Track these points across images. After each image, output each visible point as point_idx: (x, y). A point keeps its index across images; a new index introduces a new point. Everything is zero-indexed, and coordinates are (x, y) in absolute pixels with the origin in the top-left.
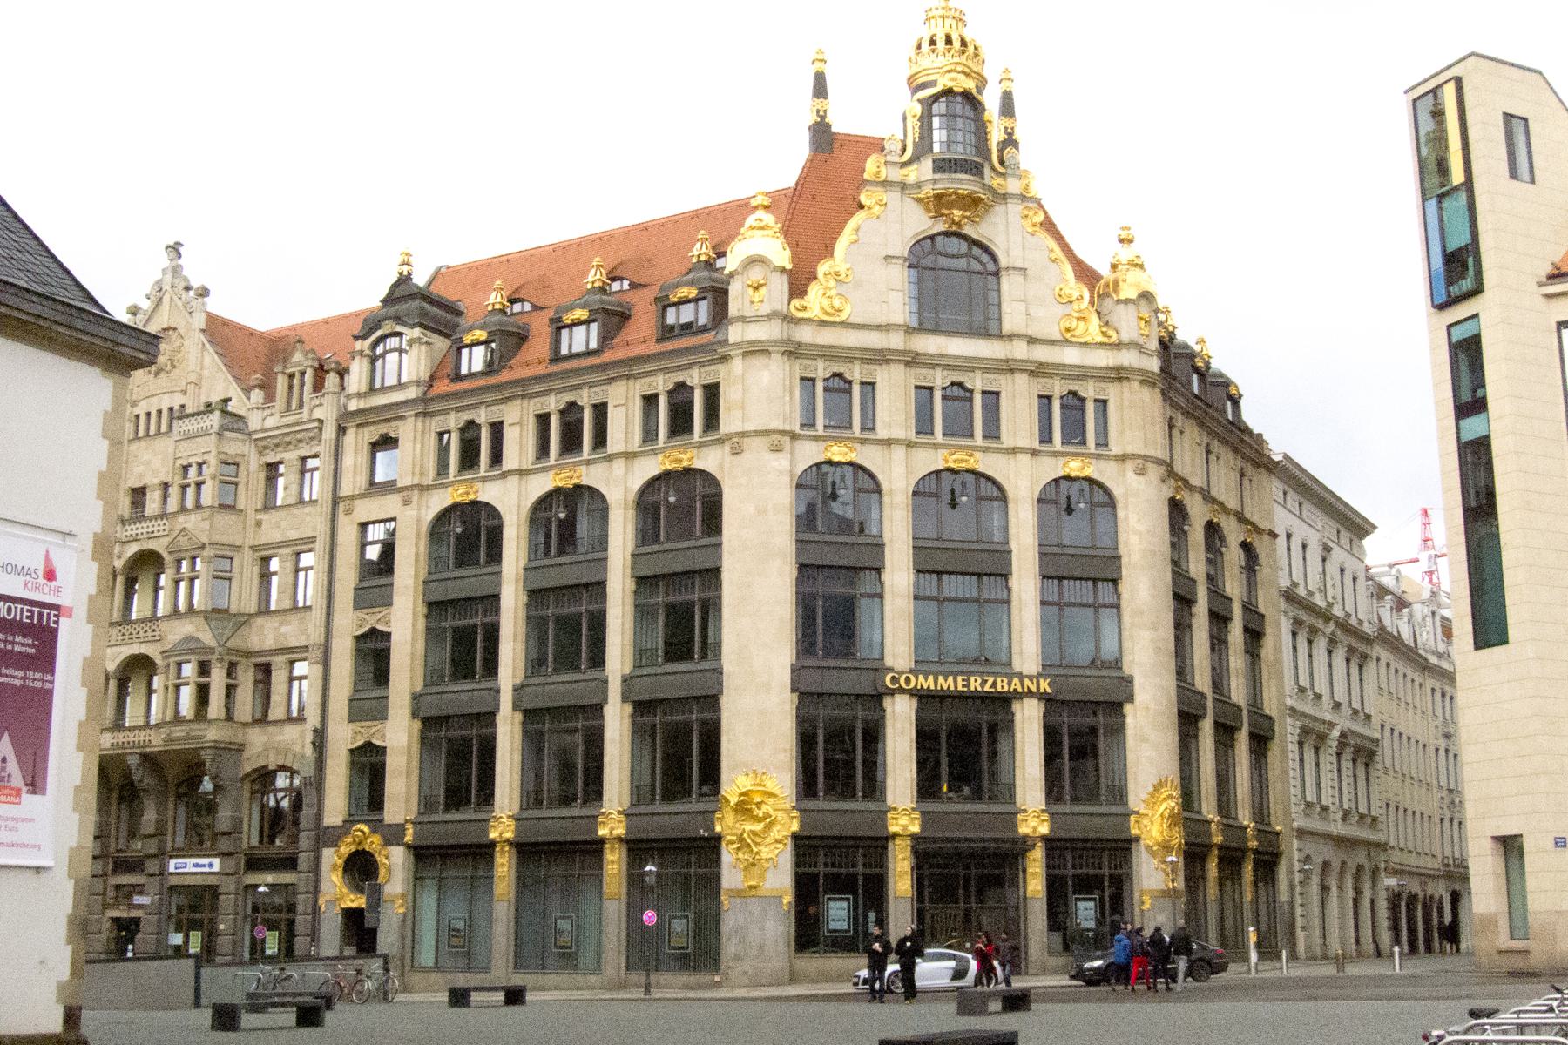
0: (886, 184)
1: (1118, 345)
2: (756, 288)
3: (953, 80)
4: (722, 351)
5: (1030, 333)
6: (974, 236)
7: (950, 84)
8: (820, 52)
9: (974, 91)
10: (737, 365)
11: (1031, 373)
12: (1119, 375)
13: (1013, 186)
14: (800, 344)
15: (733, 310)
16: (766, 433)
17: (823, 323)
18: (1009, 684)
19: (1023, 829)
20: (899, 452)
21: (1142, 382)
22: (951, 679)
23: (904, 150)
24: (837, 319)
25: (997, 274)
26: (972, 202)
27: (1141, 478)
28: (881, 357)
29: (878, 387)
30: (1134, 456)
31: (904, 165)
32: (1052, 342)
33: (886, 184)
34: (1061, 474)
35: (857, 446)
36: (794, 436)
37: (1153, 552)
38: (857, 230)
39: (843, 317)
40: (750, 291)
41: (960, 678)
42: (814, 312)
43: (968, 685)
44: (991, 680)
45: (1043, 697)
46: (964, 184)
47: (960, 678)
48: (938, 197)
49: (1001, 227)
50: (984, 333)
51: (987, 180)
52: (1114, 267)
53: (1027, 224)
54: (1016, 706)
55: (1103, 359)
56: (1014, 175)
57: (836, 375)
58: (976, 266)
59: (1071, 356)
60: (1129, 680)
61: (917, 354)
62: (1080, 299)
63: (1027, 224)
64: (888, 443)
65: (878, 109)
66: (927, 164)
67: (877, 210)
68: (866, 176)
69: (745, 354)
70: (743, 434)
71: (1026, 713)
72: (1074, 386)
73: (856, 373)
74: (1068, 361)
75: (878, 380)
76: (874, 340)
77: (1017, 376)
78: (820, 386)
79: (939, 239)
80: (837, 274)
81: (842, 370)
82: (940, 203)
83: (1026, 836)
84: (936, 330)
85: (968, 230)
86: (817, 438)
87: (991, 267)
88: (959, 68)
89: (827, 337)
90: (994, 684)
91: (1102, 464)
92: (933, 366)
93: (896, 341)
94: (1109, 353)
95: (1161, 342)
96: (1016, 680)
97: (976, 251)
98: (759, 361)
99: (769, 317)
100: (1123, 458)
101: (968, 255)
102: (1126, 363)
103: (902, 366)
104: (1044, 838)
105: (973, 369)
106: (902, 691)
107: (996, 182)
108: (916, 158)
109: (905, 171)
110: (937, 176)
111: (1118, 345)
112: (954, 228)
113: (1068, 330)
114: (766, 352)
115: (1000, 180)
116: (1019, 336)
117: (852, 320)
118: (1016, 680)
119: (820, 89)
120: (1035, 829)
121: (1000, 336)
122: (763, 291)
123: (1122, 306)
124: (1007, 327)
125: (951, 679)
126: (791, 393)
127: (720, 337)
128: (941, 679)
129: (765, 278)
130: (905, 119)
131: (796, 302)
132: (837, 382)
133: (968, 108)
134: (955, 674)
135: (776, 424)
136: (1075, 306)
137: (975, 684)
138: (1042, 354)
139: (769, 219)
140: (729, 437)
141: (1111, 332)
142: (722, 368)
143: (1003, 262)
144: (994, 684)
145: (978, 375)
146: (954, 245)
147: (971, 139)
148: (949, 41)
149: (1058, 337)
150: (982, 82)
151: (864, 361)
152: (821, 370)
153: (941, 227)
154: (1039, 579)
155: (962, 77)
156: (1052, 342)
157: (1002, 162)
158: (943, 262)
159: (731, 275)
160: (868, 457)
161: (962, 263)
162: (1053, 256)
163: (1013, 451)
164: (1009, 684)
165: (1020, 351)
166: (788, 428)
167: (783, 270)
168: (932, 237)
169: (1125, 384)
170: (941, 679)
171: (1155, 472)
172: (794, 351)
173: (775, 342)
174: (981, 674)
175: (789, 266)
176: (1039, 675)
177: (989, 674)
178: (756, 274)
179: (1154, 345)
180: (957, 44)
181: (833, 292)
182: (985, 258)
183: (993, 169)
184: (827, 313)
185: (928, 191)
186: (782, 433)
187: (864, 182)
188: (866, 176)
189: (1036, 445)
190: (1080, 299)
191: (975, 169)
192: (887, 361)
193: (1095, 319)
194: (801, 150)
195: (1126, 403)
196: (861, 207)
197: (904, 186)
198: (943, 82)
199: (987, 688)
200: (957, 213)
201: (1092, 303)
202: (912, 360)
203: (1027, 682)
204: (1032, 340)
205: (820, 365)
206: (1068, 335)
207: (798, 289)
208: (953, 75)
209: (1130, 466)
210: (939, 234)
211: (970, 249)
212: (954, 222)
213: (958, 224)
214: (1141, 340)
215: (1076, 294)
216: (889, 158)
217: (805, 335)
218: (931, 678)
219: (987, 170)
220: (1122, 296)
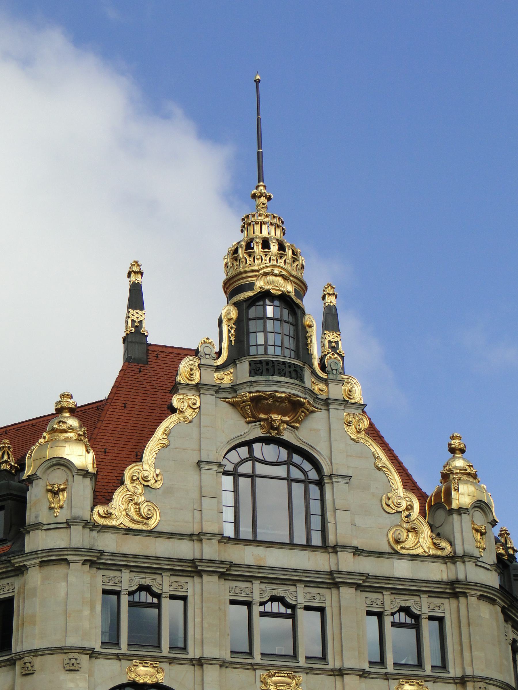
0: (198, 387)
1: (453, 559)
2: (56, 493)
3: (269, 283)
4: (17, 561)
5: (355, 543)
7: (267, 287)
8: (137, 263)
9: (292, 294)
10: (35, 577)
11: (358, 587)
12: (454, 590)
13: (336, 391)
14: (102, 552)
15: (30, 518)
16: (63, 650)
17: (128, 531)
20: (212, 673)
21: (481, 597)
23: (219, 354)
24: (145, 528)
25: (320, 484)
26: (294, 408)
28: (194, 569)
29: (190, 599)
31: (218, 368)
32: (380, 554)
33: (198, 387)
35: (165, 666)
36: (93, 654)
38: (167, 434)
39: (152, 524)
40: (50, 497)
42: (120, 520)
46: (283, 387)
48: (256, 400)
49: (323, 434)
50: (308, 546)
51: (308, 383)
52: (445, 477)
53: (351, 431)
55: (437, 572)
56: (337, 381)
57: (142, 588)
58: (296, 474)
59: (401, 569)
61: (232, 565)
62: (410, 508)
63: (351, 431)
64: (199, 663)
65: (190, 318)
66: (244, 366)
67: (189, 413)
68: (179, 379)
69: (43, 564)
70: (35, 652)
74: (398, 574)
75: (190, 593)
76: (185, 550)
77: (343, 590)
78: (125, 599)
79: (257, 447)
80: (145, 479)
81: (149, 582)
82: (255, 408)
84: (254, 542)
86: (119, 657)
87: (313, 475)
88: (276, 271)
89: (133, 546)
92: (249, 579)
93: (210, 550)
94: (443, 567)
95: (499, 556)
97: (296, 459)
98: (58, 570)
99: (68, 524)
101: (289, 463)
102: (461, 577)
103: (215, 579)
105: (294, 582)
107: (317, 387)
108: (232, 361)
109: (219, 374)
110: (253, 379)
111: (453, 559)
112: (274, 434)
113: (397, 542)
114: (67, 562)
116: (346, 547)
117: (158, 529)
119: (136, 299)
122: (63, 497)
123: (455, 517)
124: (331, 539)
126: (92, 609)
127: (15, 548)
129: (66, 483)
130: (220, 322)
131: (100, 509)
132: (144, 597)
133: (286, 312)
135: (72, 641)
139: (73, 422)
140: (21, 656)
141: (443, 544)
142: (17, 582)
143: (326, 471)
145: (301, 589)
147: (288, 342)
148: (266, 244)
149: (388, 549)
150: (302, 288)
151: (174, 572)
152: (127, 581)
153: (258, 432)
155: (280, 279)
156: (380, 554)
157: (323, 367)
158: (261, 469)
159: (31, 480)
161: (281, 471)
163: (340, 673)
165: (347, 562)
166: (86, 645)
167: (85, 473)
168: (249, 444)
169: (462, 600)
172: (96, 560)
173: (77, 551)
175: (91, 469)
178: (58, 477)
179: (492, 559)
180: (274, 248)
181: (141, 499)
182: (307, 466)
183: (314, 373)
185: (246, 393)
186: (81, 650)
187: (175, 388)
188: (179, 379)
190: (410, 508)
191: (296, 373)
192: (199, 574)
193: (426, 531)
194: (114, 361)
196: (173, 410)
197: (218, 389)
198: (260, 284)
200: (276, 417)
201: (422, 513)
202: (227, 572)
204: (358, 552)
205: (126, 575)
206: (398, 548)
207: (102, 497)
208: (270, 278)
210: (257, 440)
211: (290, 456)
212: (272, 428)
213: (277, 429)
215: (404, 504)
216: (203, 361)
217: (109, 543)
219: (307, 373)
220: (454, 506)
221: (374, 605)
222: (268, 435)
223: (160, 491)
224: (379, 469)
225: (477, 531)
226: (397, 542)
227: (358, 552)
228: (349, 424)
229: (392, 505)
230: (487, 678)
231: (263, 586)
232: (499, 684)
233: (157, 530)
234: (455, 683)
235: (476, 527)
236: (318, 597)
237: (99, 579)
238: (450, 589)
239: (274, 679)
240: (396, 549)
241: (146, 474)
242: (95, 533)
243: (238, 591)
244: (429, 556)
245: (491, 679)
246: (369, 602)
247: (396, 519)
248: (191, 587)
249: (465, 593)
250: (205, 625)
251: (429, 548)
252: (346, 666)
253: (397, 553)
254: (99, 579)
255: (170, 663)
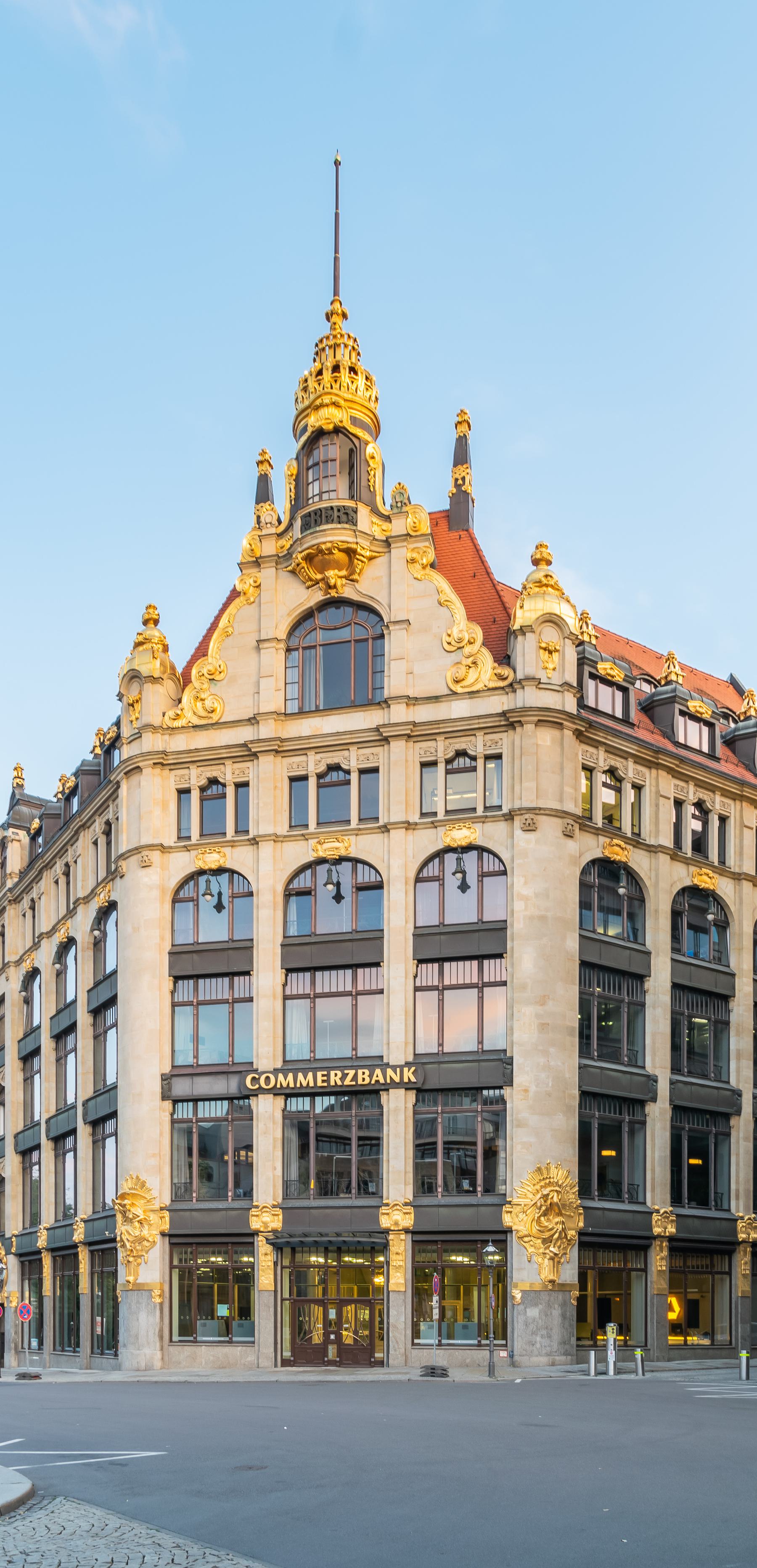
6: (355, 597)
18: (371, 1076)
19: (385, 1222)
22: (310, 1075)
24: (210, 721)
27: (531, 836)
30: (522, 811)
32: (436, 699)
34: (440, 846)
37: (543, 918)
41: (319, 1074)
43: (328, 1081)
44: (352, 1073)
45: (408, 1086)
47: (319, 1074)
54: (384, 1096)
59: (460, 709)
60: (510, 1062)
71: (392, 1105)
72: (461, 744)
73: (229, 774)
83: (387, 1232)
85: (348, 592)
90: (355, 1078)
91: (490, 827)
94: (504, 698)
96: (378, 1071)
100: (510, 817)
104: (406, 1231)
106: (261, 1091)
115: (386, 526)
118: (378, 1071)
120: (396, 1224)
121: (385, 703)
125: (310, 1075)
128: (300, 1076)
134: (315, 1070)
136: (468, 650)
137: (335, 1078)
138: (423, 714)
144: (355, 1078)
146: (333, 615)
149: (447, 692)
154: (412, 964)
160: (237, 857)
162: (443, 598)
163: (385, 829)
164: (371, 1076)
170: (300, 1076)
171: (550, 827)
174: (342, 1068)
176: (408, 1064)
177: (351, 1067)
184: (201, 717)
189: (415, 818)
195: (517, 752)
199: (347, 1082)
202: (280, 748)
203: (390, 1072)
209: (518, 821)
212: (330, 587)
214: (543, 676)
218: (290, 1076)
221: (428, 754)
222: (329, 596)
223: (225, 682)
224: (440, 604)
225: (545, 649)
226: (457, 682)
227: (412, 701)
228: (413, 561)
229: (453, 643)
230: (535, 809)
231: (319, 756)
232: (553, 813)
233: (221, 721)
234: (506, 820)
235: (543, 645)
236: (371, 757)
237: (172, 779)
238: (505, 720)
239: (326, 846)
240: (454, 689)
241: (211, 668)
242: (167, 737)
243: (295, 766)
244: (489, 689)
245: (540, 809)
246: (422, 752)
247: (454, 657)
248: (250, 771)
249: (520, 722)
250: (261, 805)
251: (490, 680)
252: (392, 821)
253: (455, 693)
254: (172, 781)
255: (232, 846)
